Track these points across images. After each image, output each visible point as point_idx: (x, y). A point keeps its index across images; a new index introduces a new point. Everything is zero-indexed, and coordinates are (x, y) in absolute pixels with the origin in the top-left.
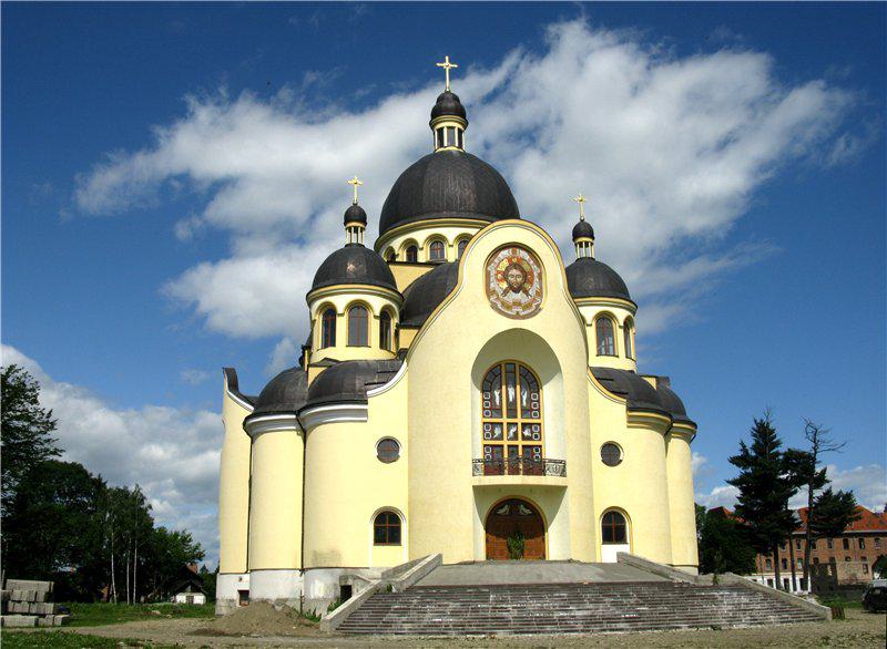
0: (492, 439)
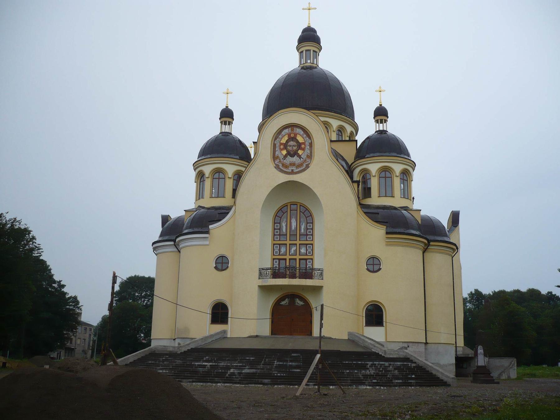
0: (279, 255)
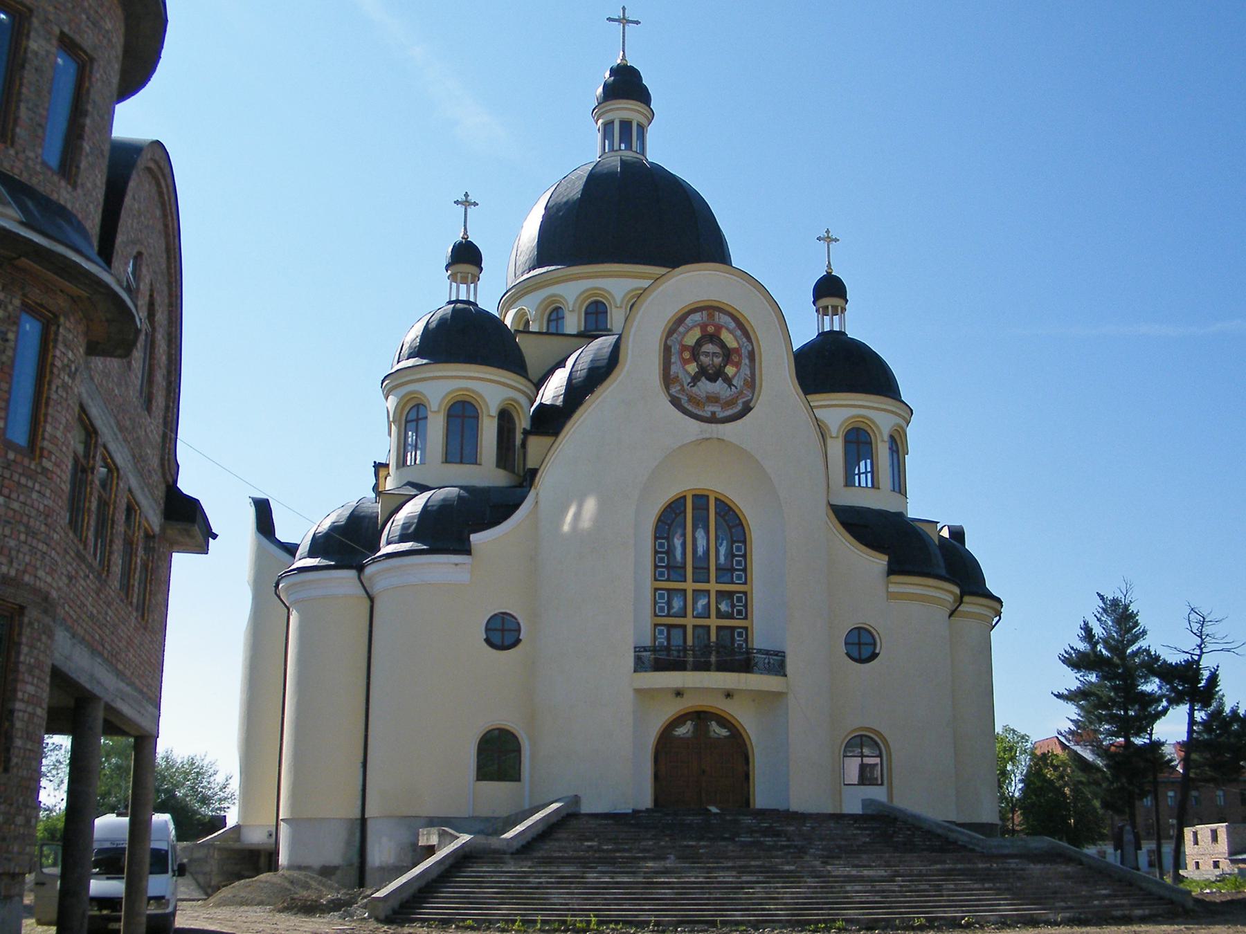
0: (668, 615)
